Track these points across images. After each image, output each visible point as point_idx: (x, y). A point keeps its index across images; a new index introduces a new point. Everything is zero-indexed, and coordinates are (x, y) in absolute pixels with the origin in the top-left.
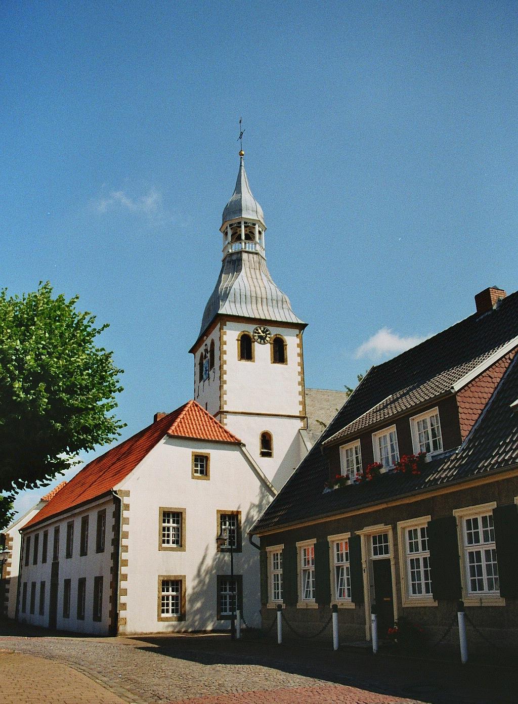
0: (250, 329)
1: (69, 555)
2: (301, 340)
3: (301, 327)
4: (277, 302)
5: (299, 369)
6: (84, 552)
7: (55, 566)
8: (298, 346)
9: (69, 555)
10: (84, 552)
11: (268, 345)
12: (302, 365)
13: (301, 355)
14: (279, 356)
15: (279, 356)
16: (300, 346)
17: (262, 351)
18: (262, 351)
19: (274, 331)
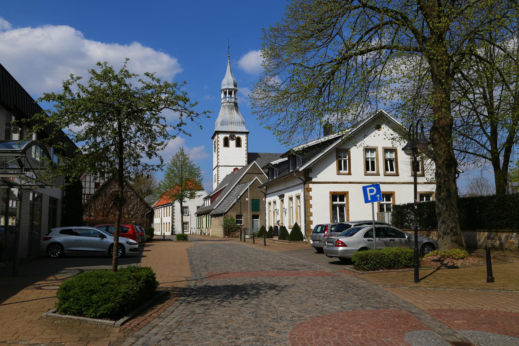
0: (228, 136)
1: (164, 217)
2: (247, 138)
3: (247, 133)
4: (238, 123)
5: (246, 149)
6: (167, 216)
7: (161, 218)
8: (246, 140)
9: (164, 217)
10: (167, 216)
11: (235, 141)
12: (247, 147)
13: (247, 144)
14: (238, 144)
15: (238, 144)
16: (247, 140)
17: (232, 143)
18: (232, 143)
19: (237, 136)
